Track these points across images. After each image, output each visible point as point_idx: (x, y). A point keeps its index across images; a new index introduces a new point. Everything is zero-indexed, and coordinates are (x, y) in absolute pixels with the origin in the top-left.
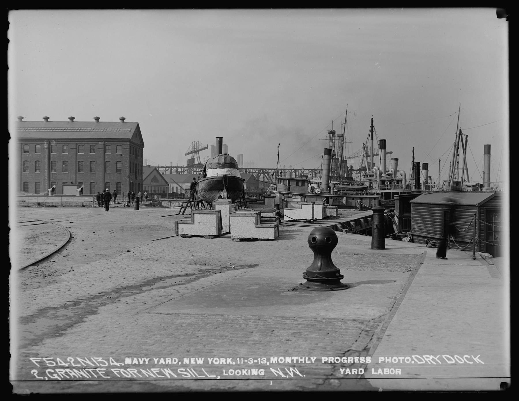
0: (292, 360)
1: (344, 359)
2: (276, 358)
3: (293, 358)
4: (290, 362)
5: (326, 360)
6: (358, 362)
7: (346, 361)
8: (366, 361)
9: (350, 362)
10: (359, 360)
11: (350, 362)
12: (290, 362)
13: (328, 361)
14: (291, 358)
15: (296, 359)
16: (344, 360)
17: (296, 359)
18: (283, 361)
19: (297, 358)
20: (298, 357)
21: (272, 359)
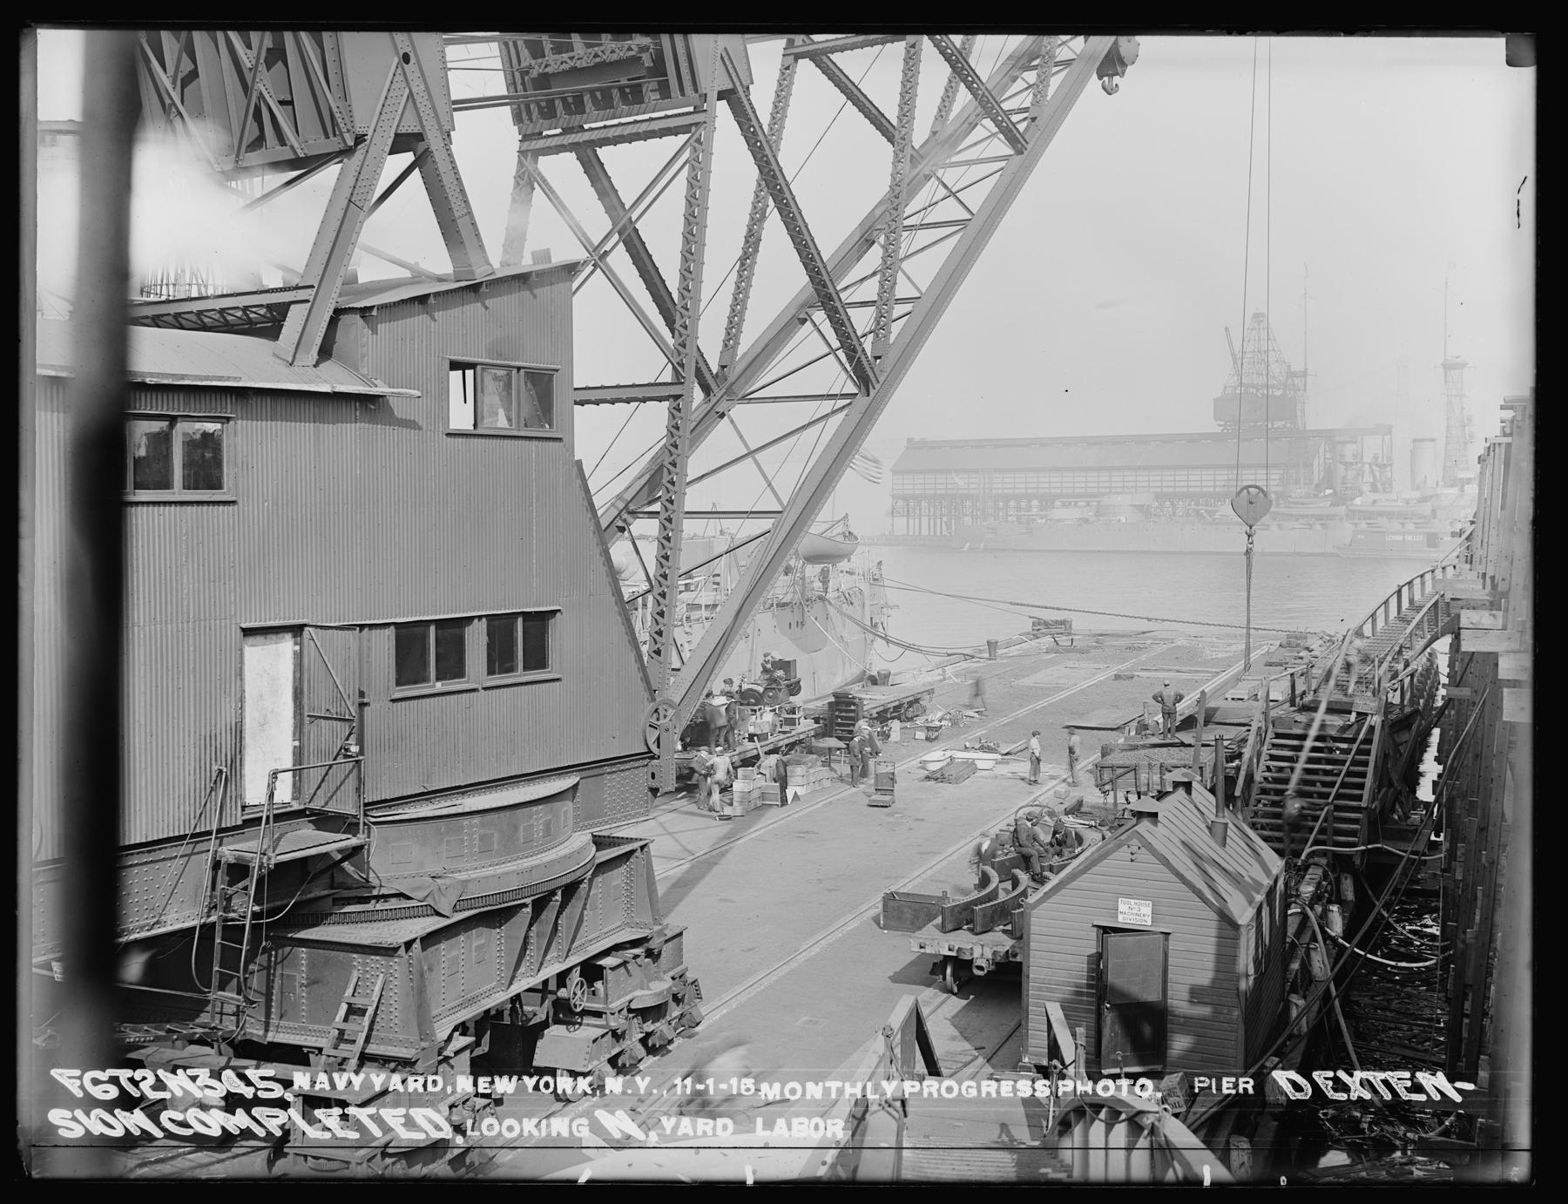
0: (827, 1091)
1: (969, 1087)
2: (777, 1086)
3: (828, 1084)
4: (818, 1096)
5: (917, 1089)
6: (1012, 1095)
7: (974, 1093)
8: (1034, 1090)
9: (988, 1094)
10: (1015, 1090)
11: (988, 1094)
12: (818, 1096)
13: (922, 1089)
14: (821, 1084)
15: (838, 1089)
16: (970, 1090)
17: (838, 1089)
18: (798, 1095)
19: (839, 1084)
20: (844, 1082)
21: (764, 1087)
